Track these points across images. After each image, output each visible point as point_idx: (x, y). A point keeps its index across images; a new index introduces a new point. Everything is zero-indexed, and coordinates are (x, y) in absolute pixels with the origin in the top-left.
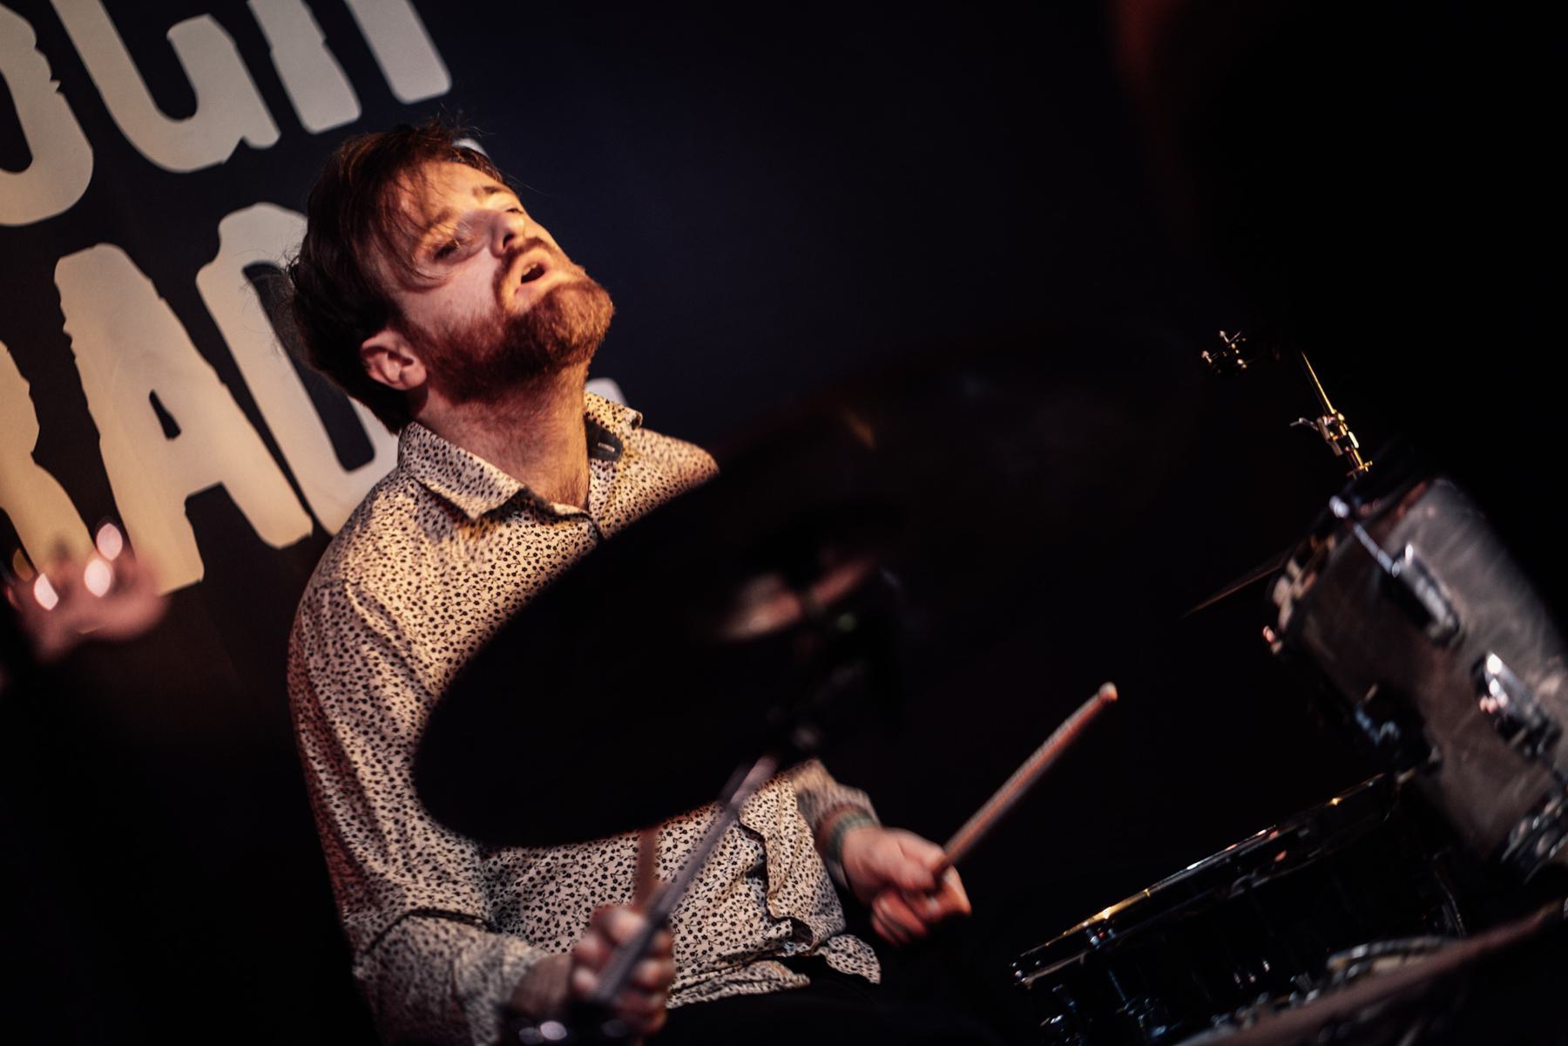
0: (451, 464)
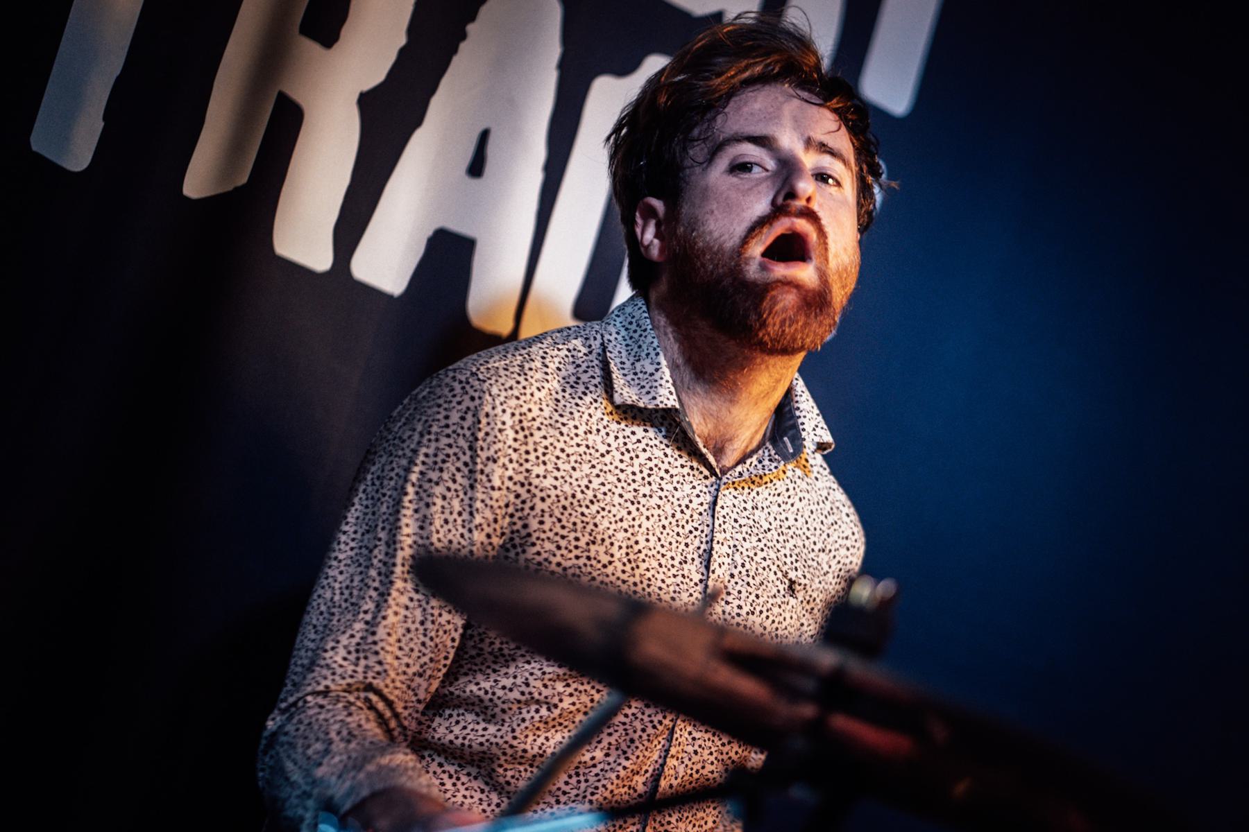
0: (640, 347)
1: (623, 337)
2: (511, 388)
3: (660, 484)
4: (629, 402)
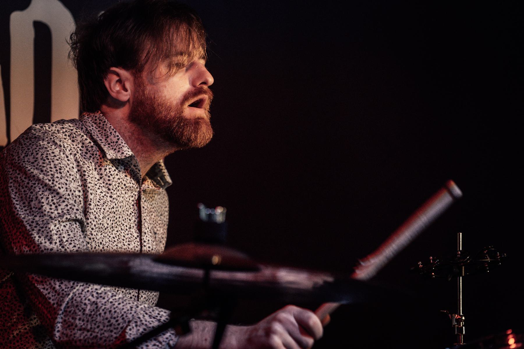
0: (105, 130)
1: (95, 127)
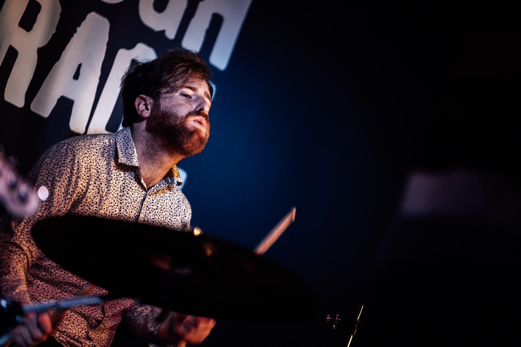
0: (128, 145)
2: (86, 154)
3: (128, 192)
4: (123, 163)
